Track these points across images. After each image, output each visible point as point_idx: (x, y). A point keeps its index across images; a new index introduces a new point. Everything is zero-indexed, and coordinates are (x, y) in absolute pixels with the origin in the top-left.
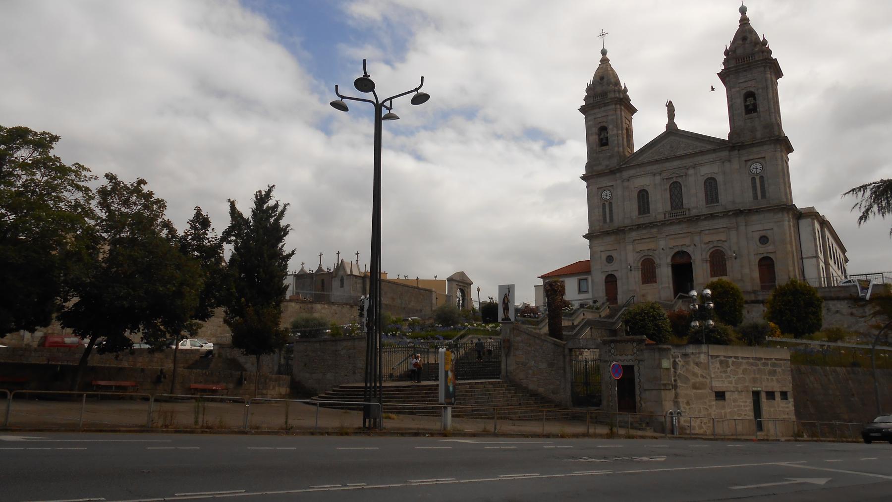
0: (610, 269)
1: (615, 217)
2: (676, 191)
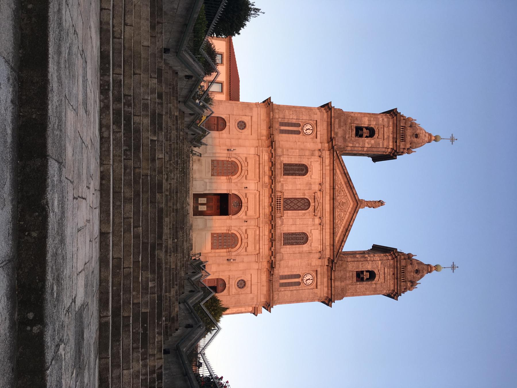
0: (232, 124)
1: (285, 136)
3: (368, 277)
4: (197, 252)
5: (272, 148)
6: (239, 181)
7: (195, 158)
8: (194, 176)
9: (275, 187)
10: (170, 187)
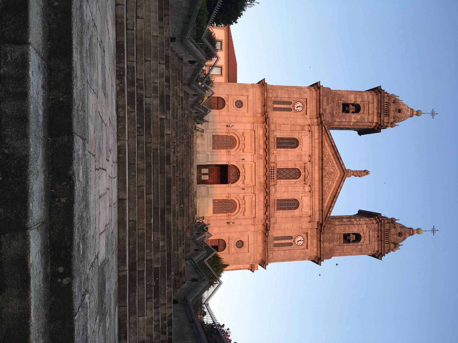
0: (230, 104)
1: (277, 113)
3: (354, 239)
4: (201, 216)
5: (266, 124)
6: (237, 153)
7: (198, 133)
8: (198, 150)
9: (269, 158)
10: (177, 159)
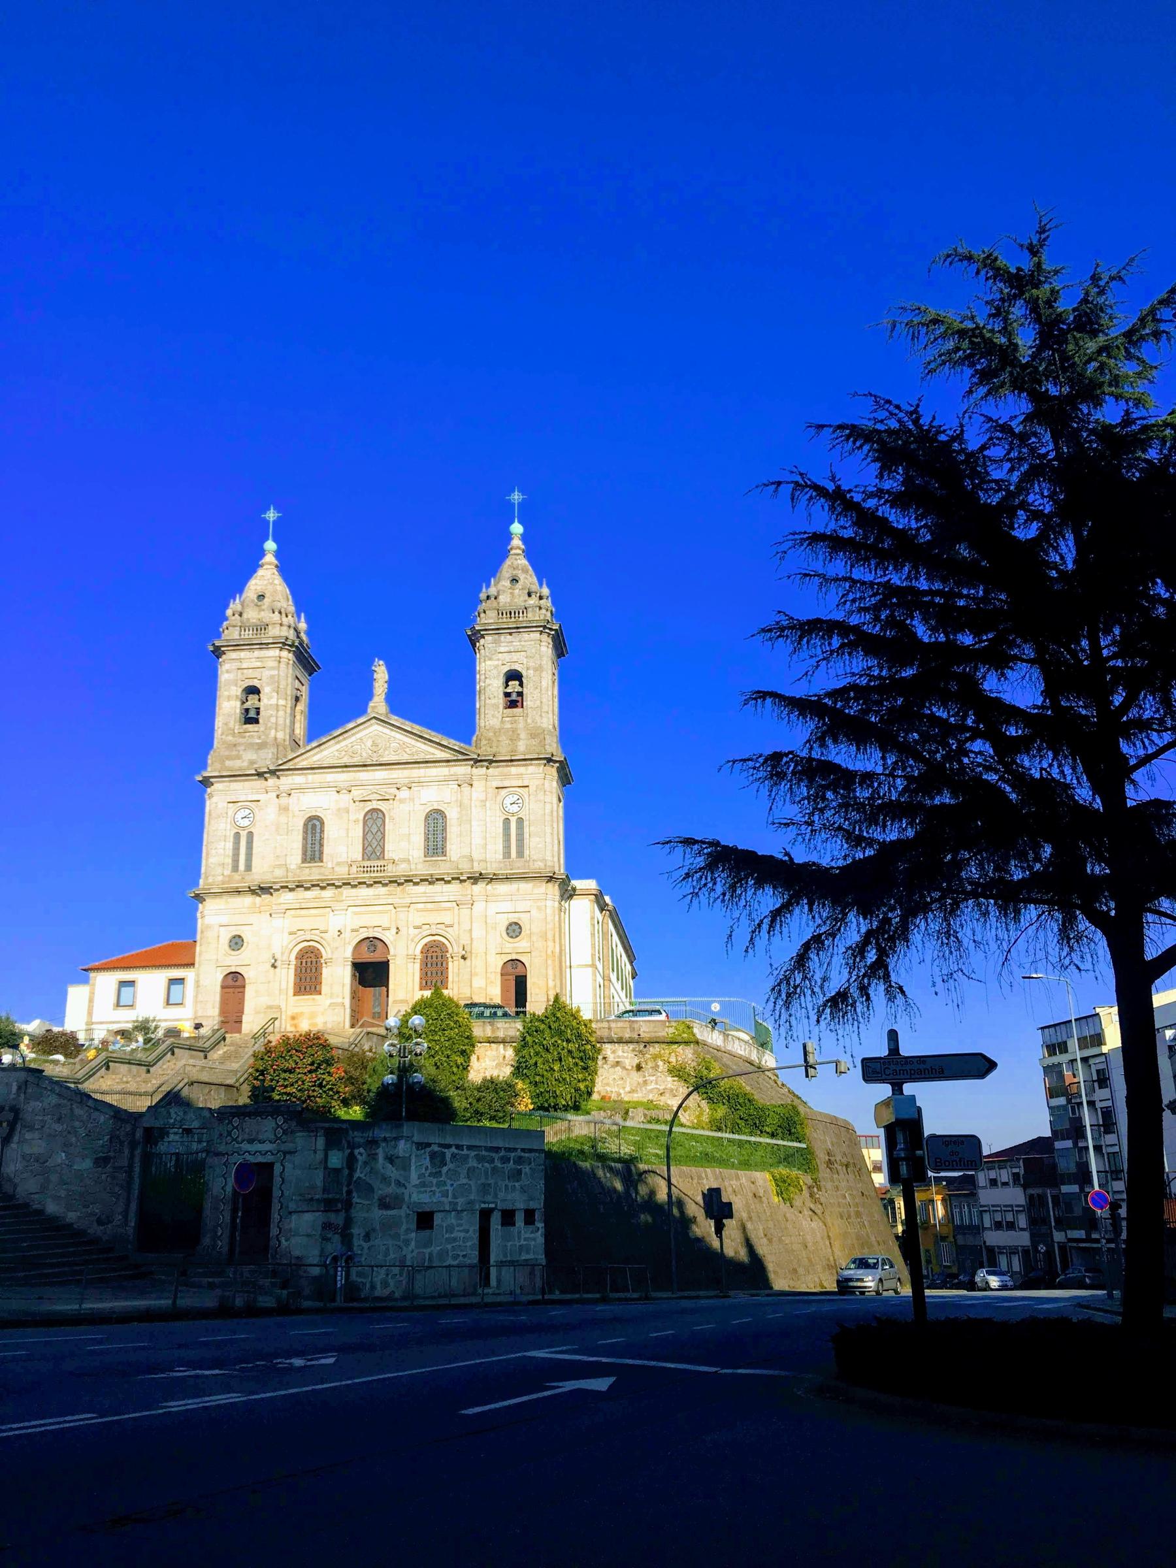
0: (234, 961)
2: (374, 823)
